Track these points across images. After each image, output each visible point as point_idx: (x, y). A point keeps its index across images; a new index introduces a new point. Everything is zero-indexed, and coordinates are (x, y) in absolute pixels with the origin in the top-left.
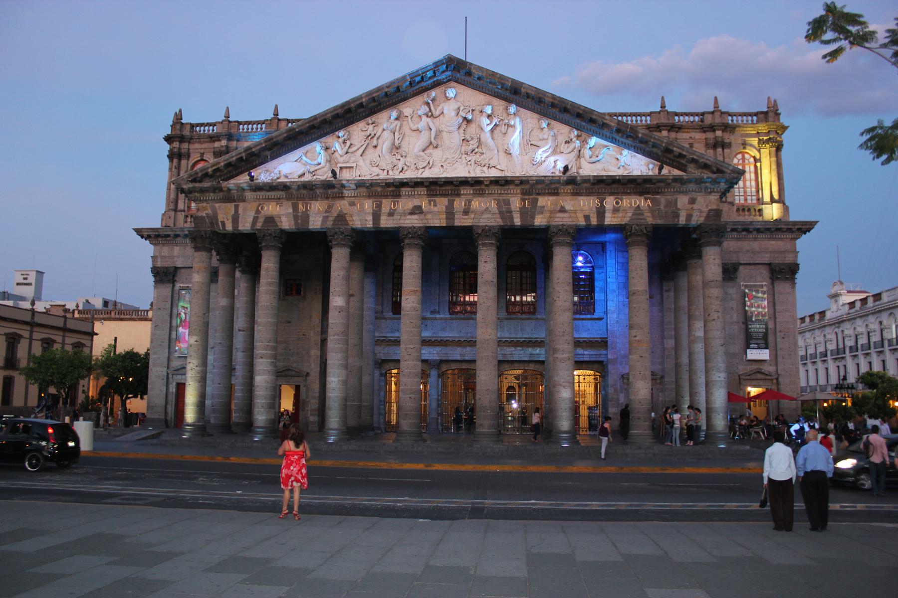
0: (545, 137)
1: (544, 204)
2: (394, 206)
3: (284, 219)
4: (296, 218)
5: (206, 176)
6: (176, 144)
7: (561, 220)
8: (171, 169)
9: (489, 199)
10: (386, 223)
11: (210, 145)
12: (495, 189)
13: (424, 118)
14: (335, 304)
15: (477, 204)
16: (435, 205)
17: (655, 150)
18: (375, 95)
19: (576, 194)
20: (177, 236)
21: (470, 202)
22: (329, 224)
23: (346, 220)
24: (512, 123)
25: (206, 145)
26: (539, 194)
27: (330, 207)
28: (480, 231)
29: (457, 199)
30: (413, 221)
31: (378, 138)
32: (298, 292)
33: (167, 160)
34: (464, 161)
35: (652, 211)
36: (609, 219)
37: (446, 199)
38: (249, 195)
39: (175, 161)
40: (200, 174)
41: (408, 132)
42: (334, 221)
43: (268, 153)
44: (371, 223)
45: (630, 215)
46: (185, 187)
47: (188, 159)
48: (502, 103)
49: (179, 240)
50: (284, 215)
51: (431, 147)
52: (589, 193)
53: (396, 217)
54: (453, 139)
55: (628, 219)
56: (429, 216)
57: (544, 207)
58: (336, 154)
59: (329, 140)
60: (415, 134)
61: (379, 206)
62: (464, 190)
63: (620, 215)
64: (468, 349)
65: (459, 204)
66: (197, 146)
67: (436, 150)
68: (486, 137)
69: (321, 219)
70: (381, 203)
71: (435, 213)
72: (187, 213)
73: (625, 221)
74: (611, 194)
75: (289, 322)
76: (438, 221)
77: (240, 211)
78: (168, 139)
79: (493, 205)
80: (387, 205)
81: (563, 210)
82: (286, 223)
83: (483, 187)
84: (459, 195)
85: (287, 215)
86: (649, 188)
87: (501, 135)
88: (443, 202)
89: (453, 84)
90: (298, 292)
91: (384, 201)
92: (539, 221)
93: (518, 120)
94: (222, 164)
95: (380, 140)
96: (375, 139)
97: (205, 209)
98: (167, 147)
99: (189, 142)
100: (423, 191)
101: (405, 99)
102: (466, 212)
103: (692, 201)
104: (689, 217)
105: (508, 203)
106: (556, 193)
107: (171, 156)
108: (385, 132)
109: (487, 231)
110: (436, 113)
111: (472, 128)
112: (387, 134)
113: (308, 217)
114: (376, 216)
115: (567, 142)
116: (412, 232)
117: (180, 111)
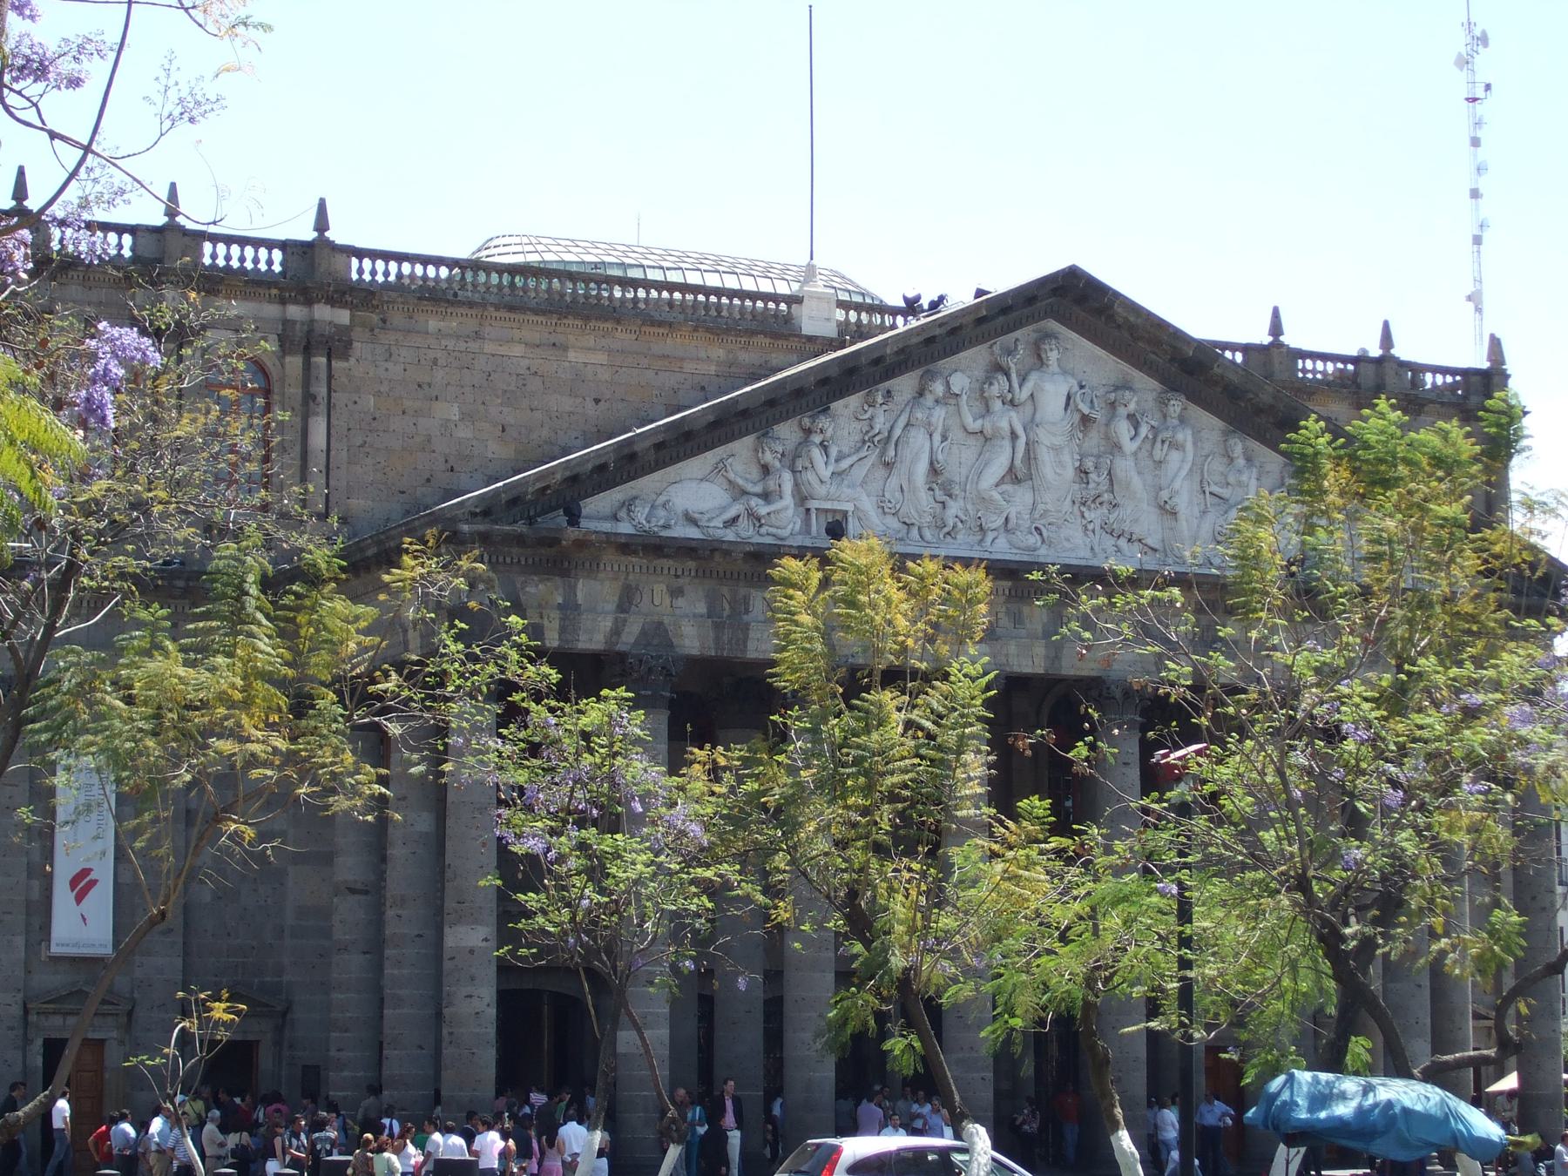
13: (997, 405)
24: (1180, 436)
28: (1118, 694)
34: (1079, 519)
41: (956, 434)
46: (465, 528)
48: (1153, 384)
58: (810, 476)
60: (971, 441)
68: (1124, 467)
82: (692, 640)
87: (1150, 463)
89: (1052, 325)
93: (1189, 432)
95: (906, 453)
108: (913, 432)
110: (1023, 395)
111: (1094, 441)
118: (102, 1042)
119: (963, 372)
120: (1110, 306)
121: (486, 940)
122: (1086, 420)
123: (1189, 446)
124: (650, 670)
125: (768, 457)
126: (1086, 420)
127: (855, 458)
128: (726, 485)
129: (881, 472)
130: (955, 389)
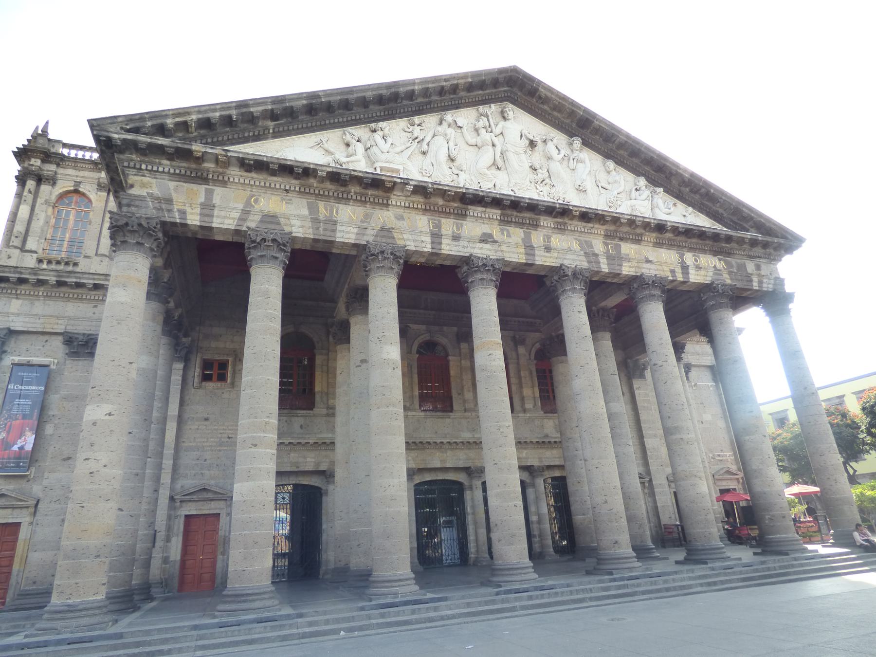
0: (617, 178)
1: (628, 252)
2: (458, 229)
3: (294, 222)
4: (316, 221)
5: (161, 130)
6: (36, 162)
7: (649, 271)
8: (19, 195)
9: (570, 238)
10: (449, 248)
11: (95, 175)
12: (578, 225)
13: (483, 131)
14: (385, 356)
15: (558, 241)
16: (509, 236)
17: (721, 211)
18: (430, 86)
19: (658, 244)
20: (22, 281)
21: (549, 237)
22: (368, 238)
23: (394, 238)
25: (86, 174)
26: (621, 239)
27: (367, 216)
28: (570, 273)
29: (533, 232)
30: (482, 251)
31: (428, 144)
32: (222, 378)
33: (14, 186)
35: (730, 273)
36: (695, 277)
37: (521, 230)
38: (235, 173)
39: (31, 184)
40: (149, 124)
42: (376, 236)
43: (271, 124)
44: (429, 246)
45: (711, 274)
46: (116, 136)
47: (54, 184)
49: (23, 287)
50: (296, 217)
51: (493, 168)
52: (671, 245)
53: (462, 243)
54: (520, 160)
55: (710, 279)
56: (504, 248)
57: (628, 255)
58: (374, 149)
59: (360, 131)
61: (438, 226)
62: (546, 222)
63: (702, 272)
64: (449, 453)
65: (537, 238)
66: (70, 171)
67: (499, 172)
68: (555, 166)
69: (355, 230)
70: (440, 222)
71: (510, 246)
72: (41, 254)
73: (708, 280)
74: (691, 249)
75: (206, 419)
76: (515, 255)
77: (216, 200)
78: (22, 154)
79: (576, 246)
80: (448, 225)
81: (648, 261)
83: (566, 220)
84: (536, 226)
85: (301, 218)
86: (723, 248)
88: (517, 234)
90: (222, 378)
91: (443, 220)
92: (627, 270)
94: (194, 117)
96: (425, 143)
97: (143, 185)
98: (14, 167)
99: (58, 165)
100: (496, 213)
101: (456, 106)
102: (548, 249)
103: (758, 267)
104: (760, 282)
105: (591, 246)
106: (638, 241)
107: (21, 179)
109: (576, 274)
111: (537, 157)
112: (440, 141)
113: (335, 223)
114: (436, 236)
115: (636, 190)
116: (486, 266)
117: (47, 123)
118: (19, 524)
119: (465, 117)
120: (536, 90)
121: (110, 414)
122: (532, 144)
123: (587, 160)
124: (264, 240)
125: (348, 138)
126: (532, 144)
127: (404, 147)
128: (324, 152)
129: (421, 157)
130: (460, 124)
